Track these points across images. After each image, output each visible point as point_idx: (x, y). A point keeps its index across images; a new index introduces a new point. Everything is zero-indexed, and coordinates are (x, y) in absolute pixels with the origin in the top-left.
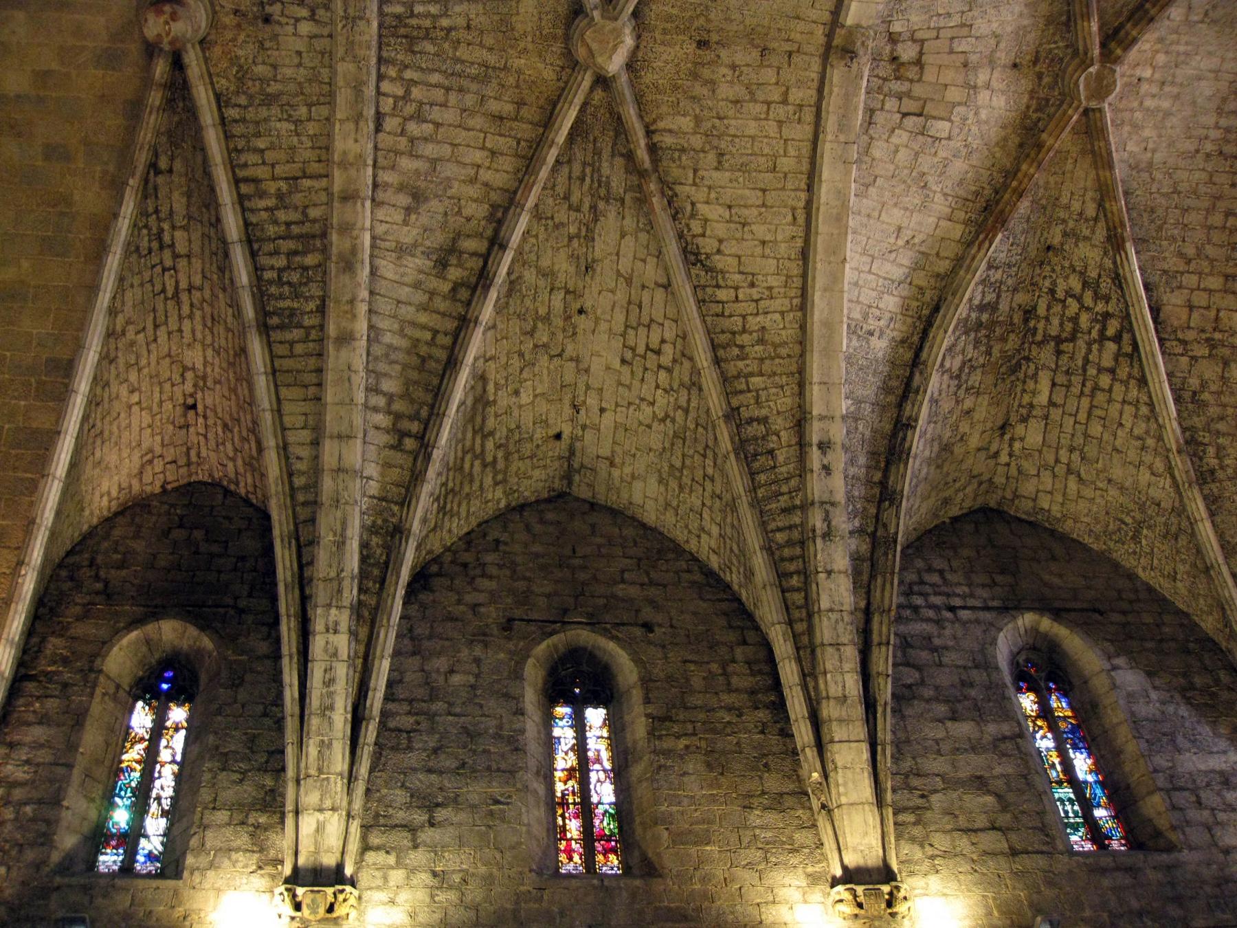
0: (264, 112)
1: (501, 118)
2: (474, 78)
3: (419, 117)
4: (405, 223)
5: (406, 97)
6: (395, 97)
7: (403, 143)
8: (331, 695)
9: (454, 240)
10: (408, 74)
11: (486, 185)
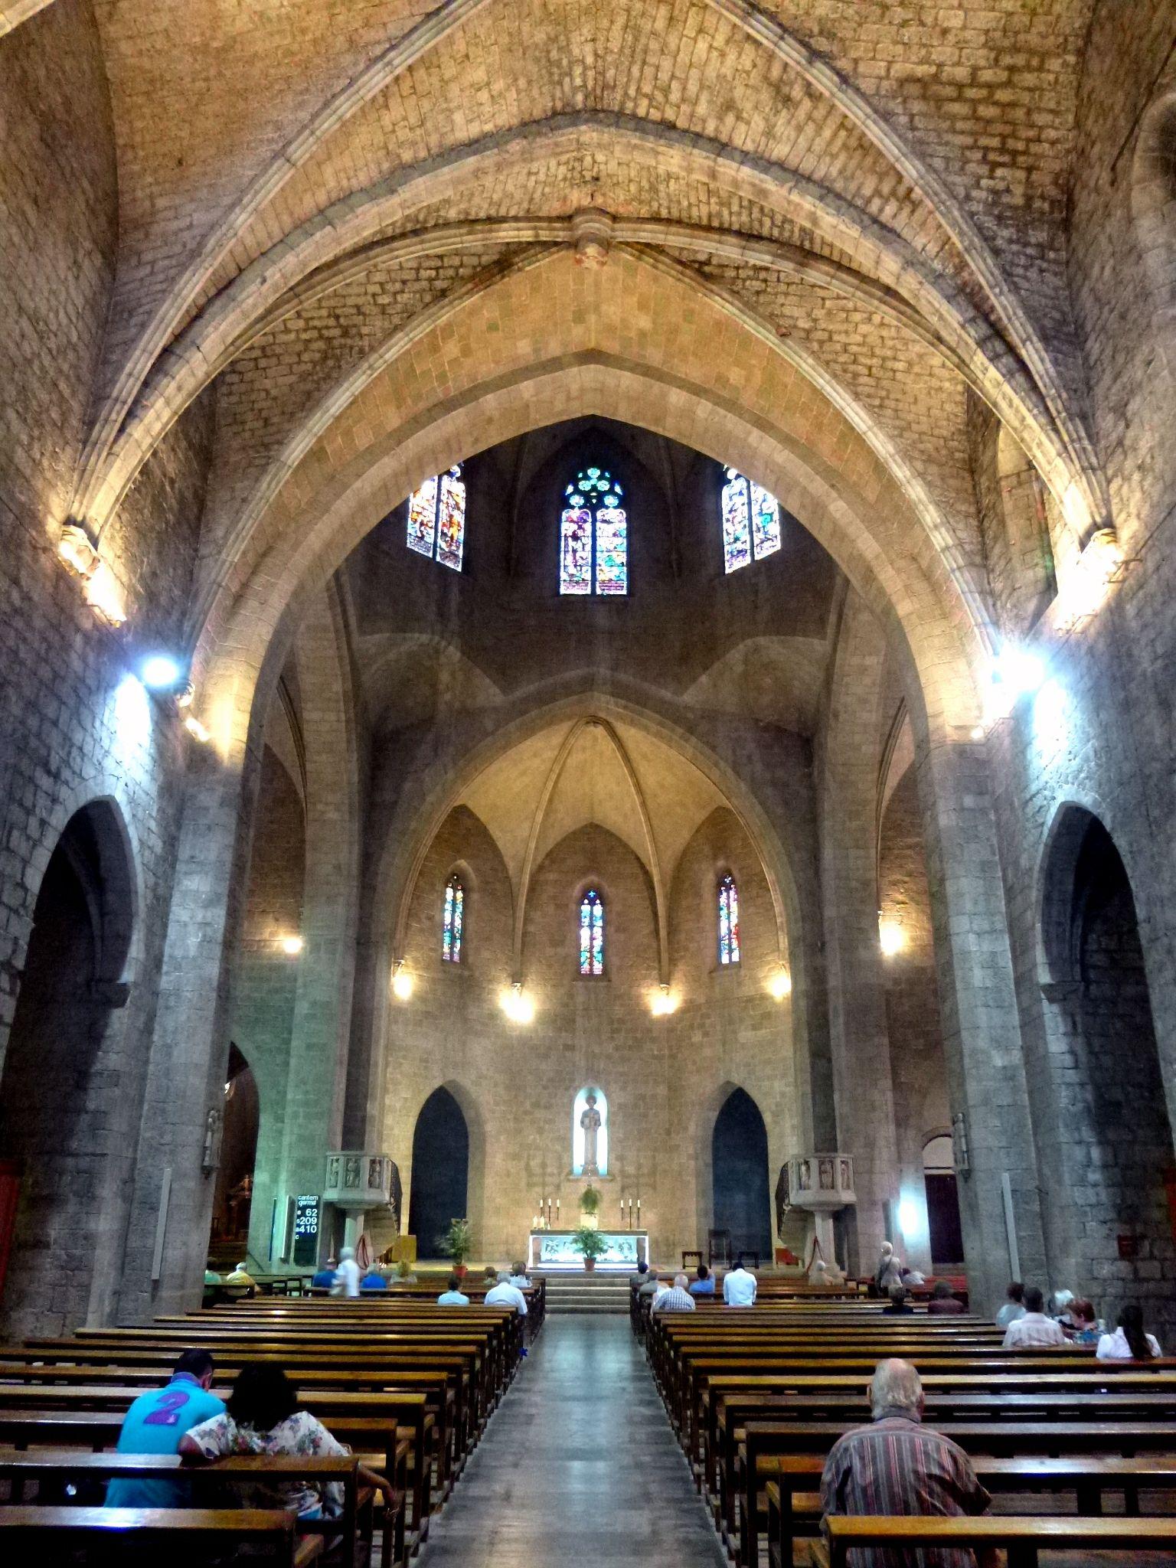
0: (662, 195)
1: (671, 19)
2: (636, 39)
3: (666, 91)
4: (748, 123)
5: (651, 98)
6: (650, 106)
7: (684, 108)
8: (1017, 411)
9: (770, 84)
10: (632, 92)
11: (727, 42)
